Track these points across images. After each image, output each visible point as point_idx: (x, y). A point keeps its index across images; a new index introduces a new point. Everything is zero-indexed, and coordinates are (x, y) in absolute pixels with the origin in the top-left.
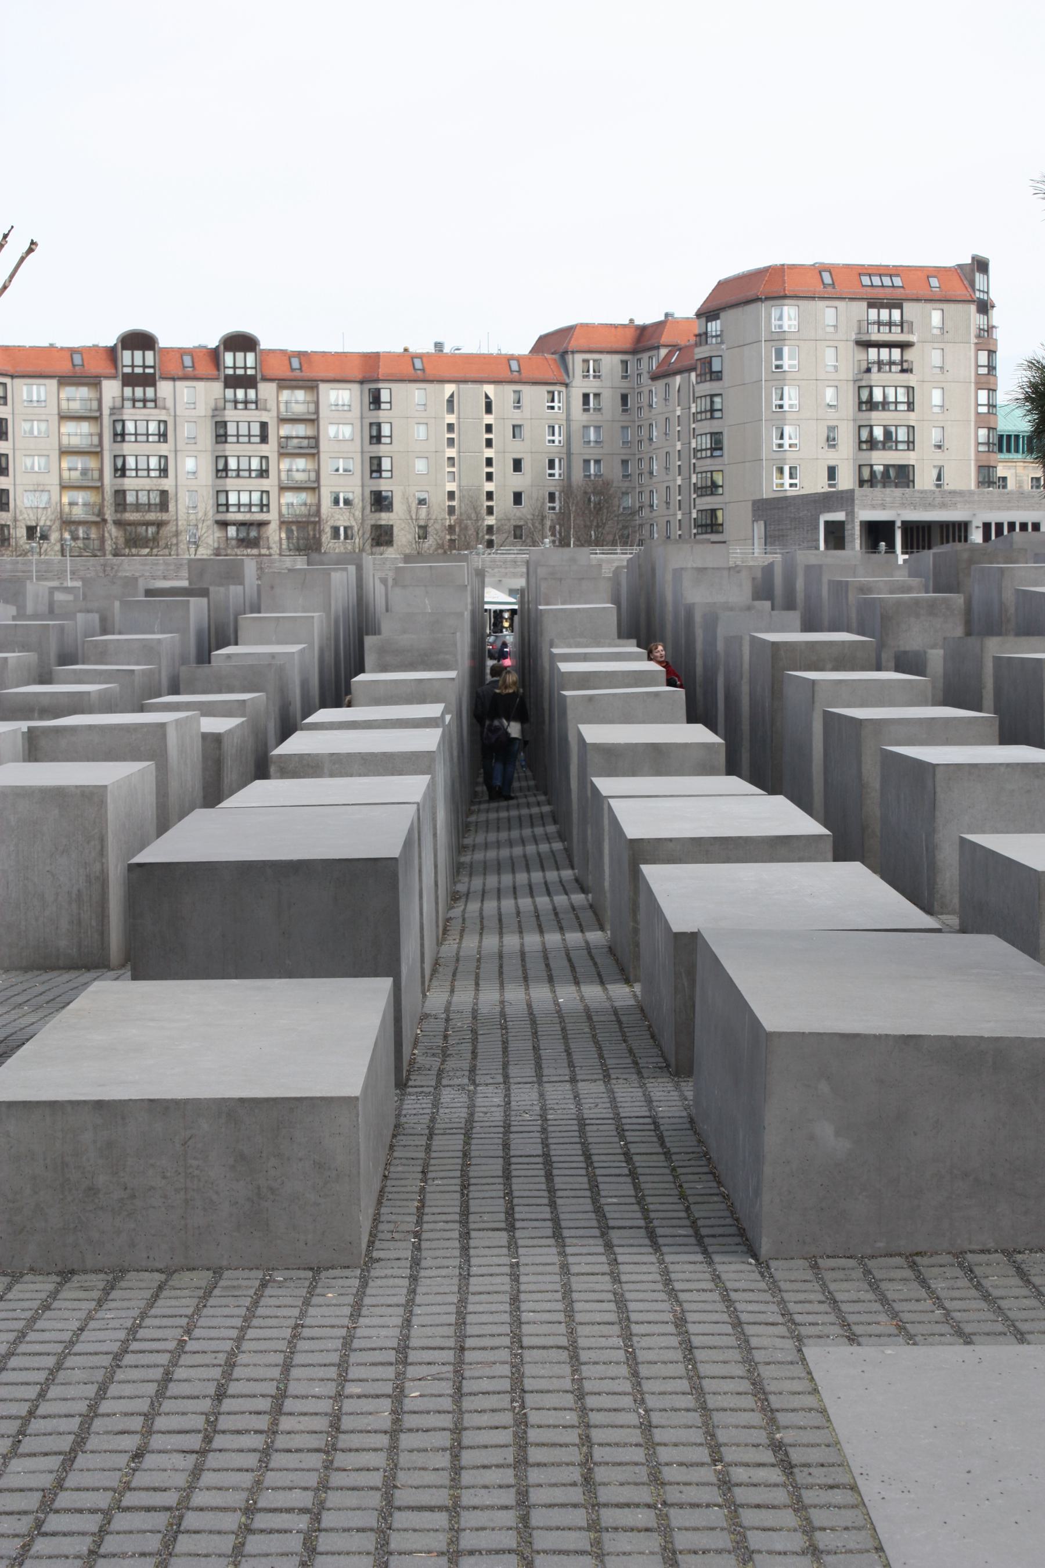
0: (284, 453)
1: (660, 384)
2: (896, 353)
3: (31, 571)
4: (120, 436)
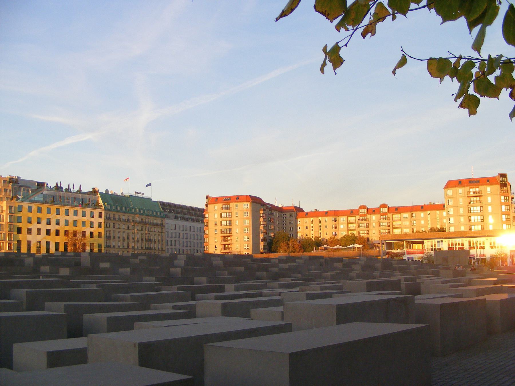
2: (478, 198)
4: (359, 227)
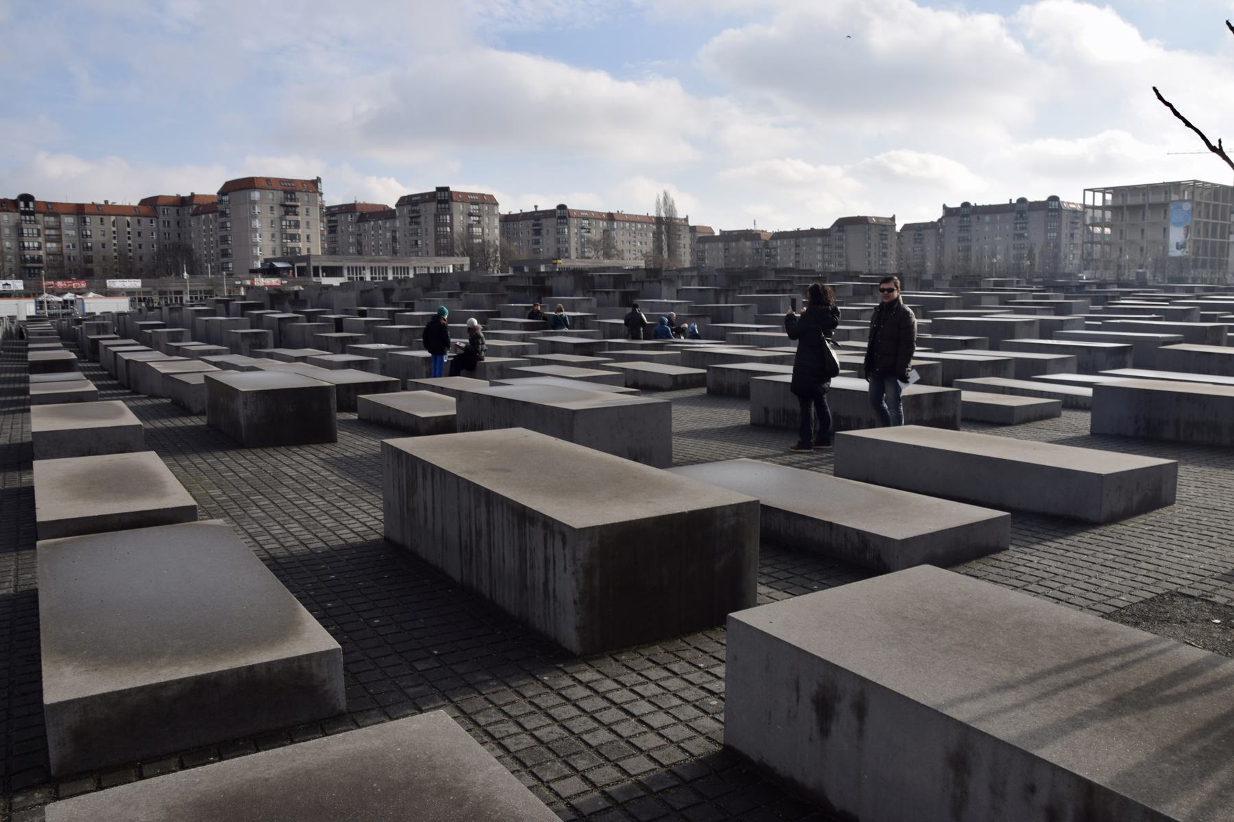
0: (47, 241)
1: (195, 218)
3: (1214, 243)
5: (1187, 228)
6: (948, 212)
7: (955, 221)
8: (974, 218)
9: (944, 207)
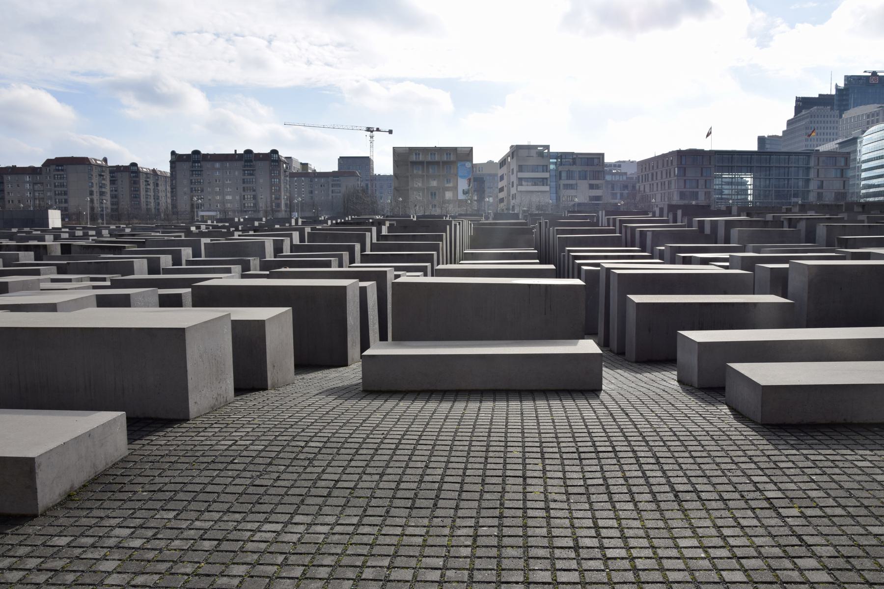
5: (470, 180)
6: (177, 159)
7: (186, 166)
8: (207, 165)
9: (173, 153)
